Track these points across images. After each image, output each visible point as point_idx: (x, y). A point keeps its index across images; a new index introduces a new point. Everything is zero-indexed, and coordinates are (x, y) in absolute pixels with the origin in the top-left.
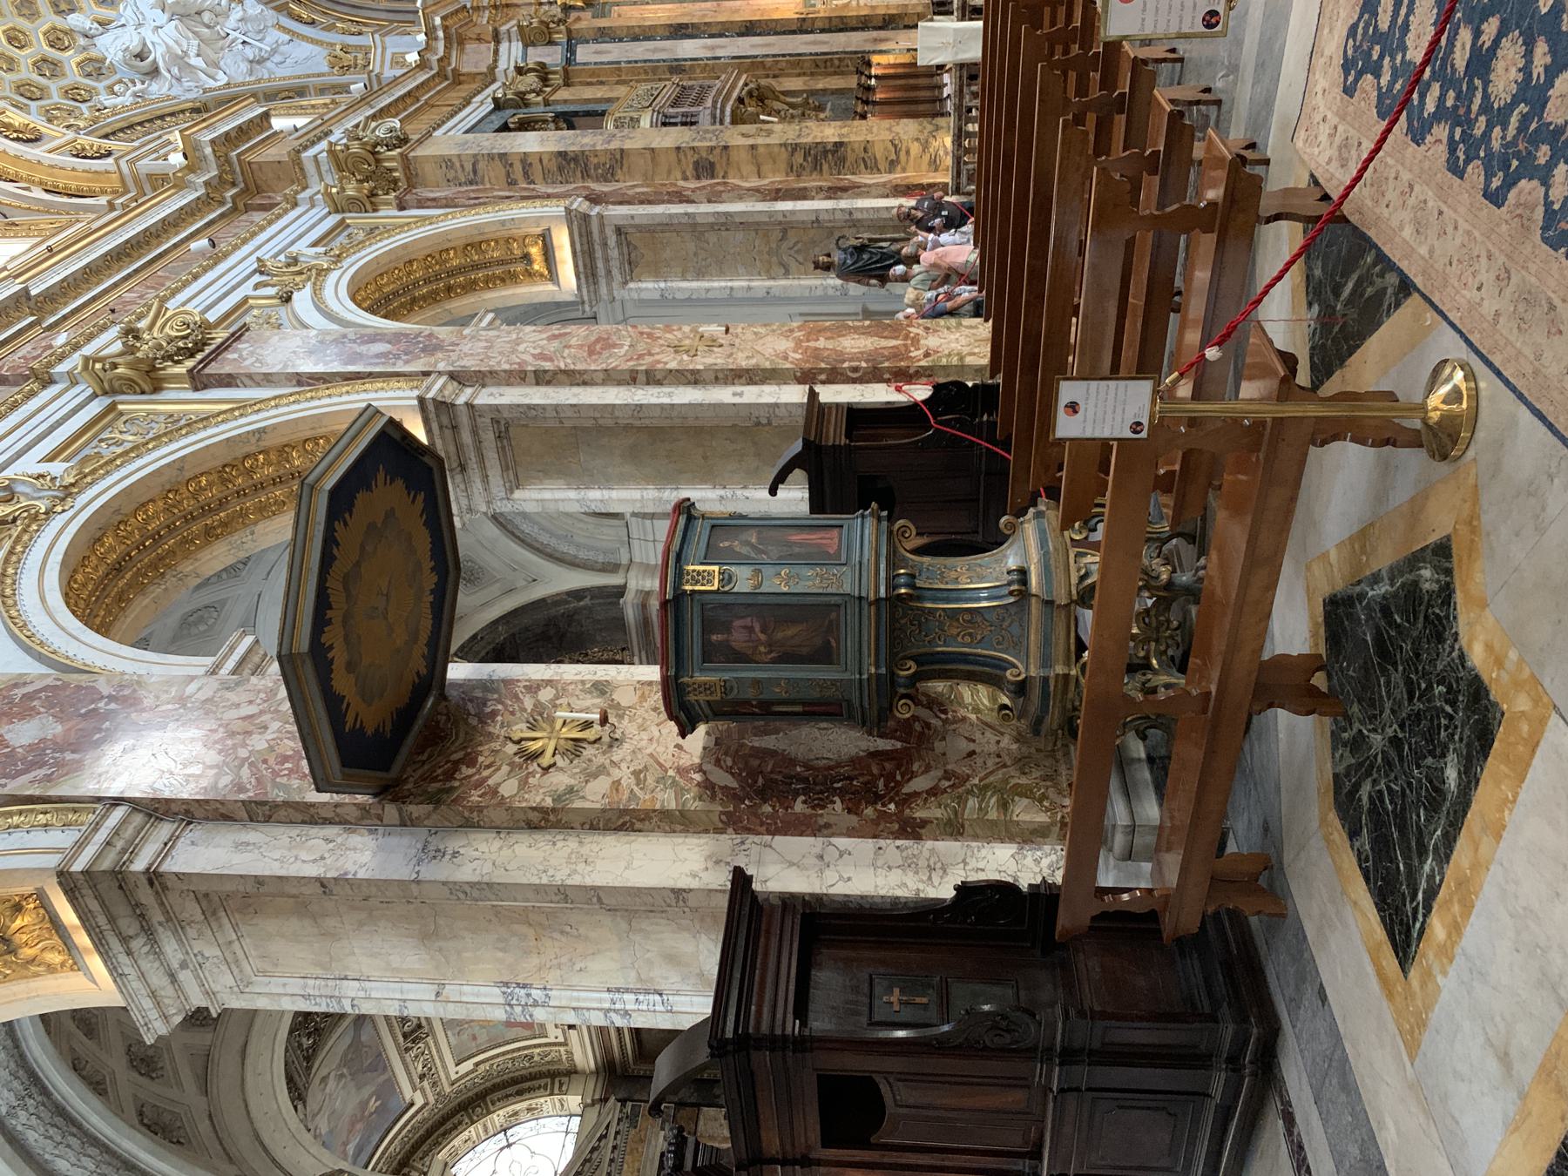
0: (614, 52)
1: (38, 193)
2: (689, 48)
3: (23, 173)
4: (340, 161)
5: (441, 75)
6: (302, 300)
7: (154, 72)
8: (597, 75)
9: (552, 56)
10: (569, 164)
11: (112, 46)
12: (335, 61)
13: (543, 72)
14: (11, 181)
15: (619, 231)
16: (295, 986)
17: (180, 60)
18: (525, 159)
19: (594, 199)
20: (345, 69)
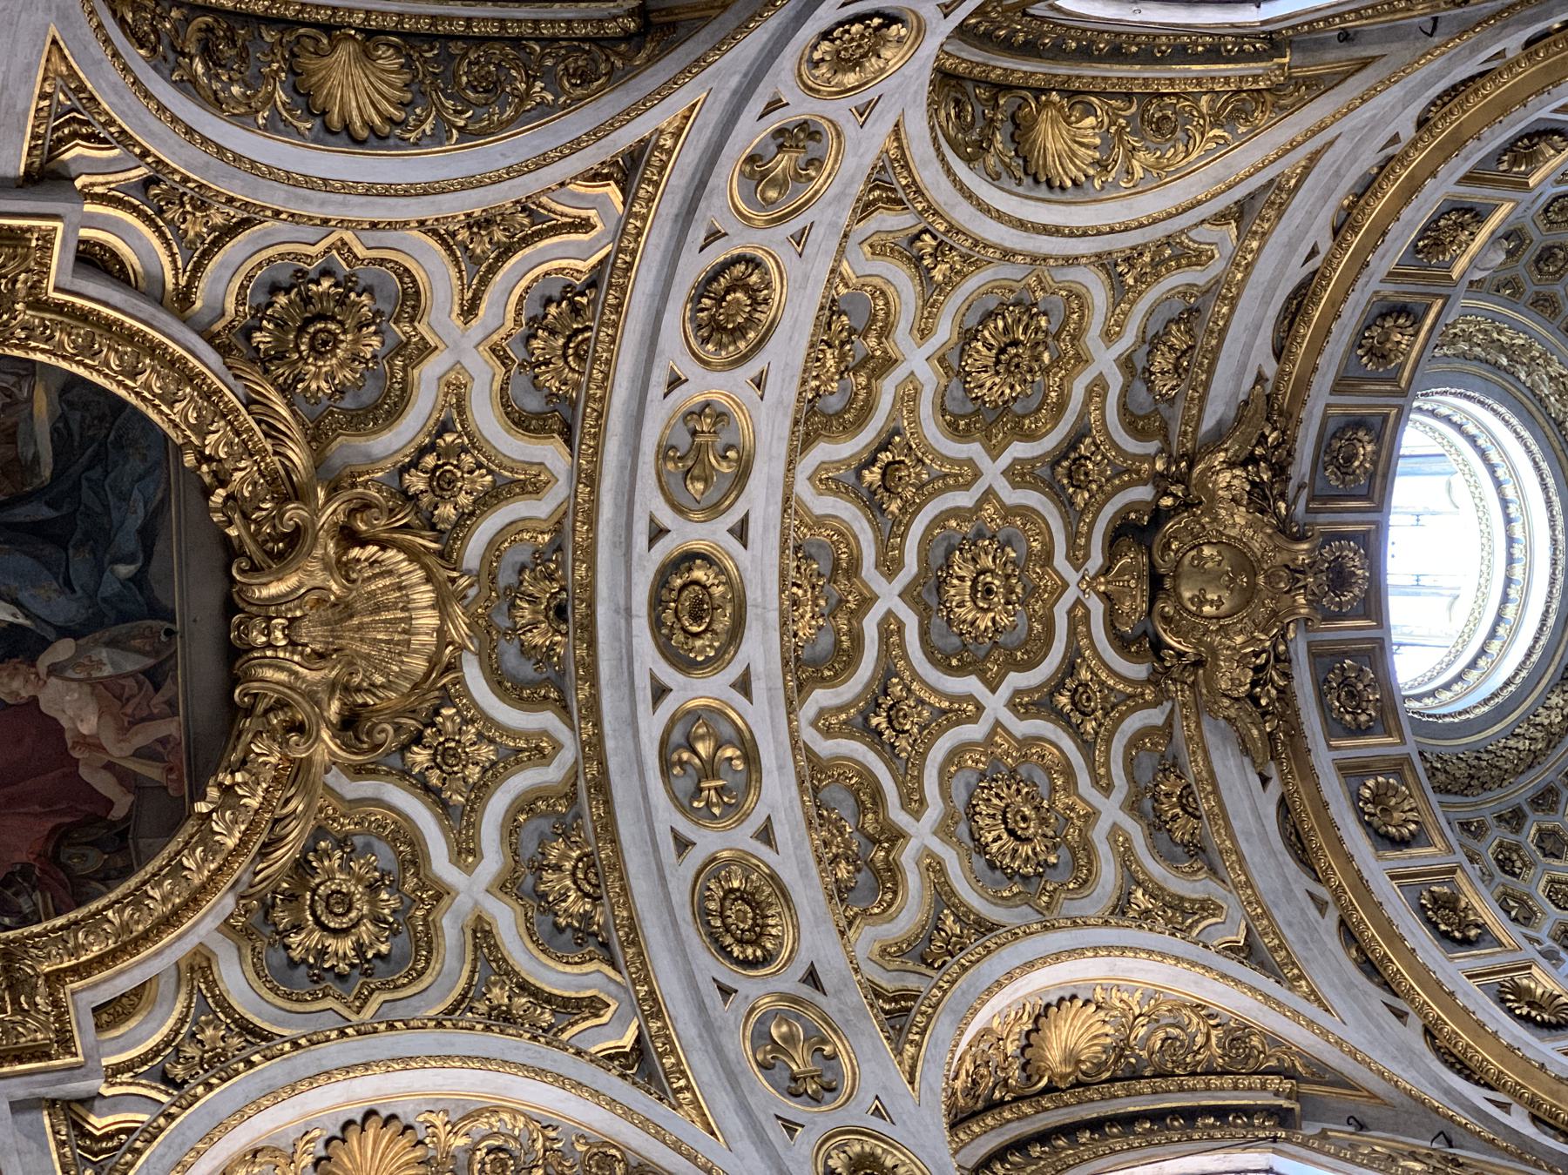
1: (1519, 1121)
3: (1511, 1077)
14: (1488, 1086)
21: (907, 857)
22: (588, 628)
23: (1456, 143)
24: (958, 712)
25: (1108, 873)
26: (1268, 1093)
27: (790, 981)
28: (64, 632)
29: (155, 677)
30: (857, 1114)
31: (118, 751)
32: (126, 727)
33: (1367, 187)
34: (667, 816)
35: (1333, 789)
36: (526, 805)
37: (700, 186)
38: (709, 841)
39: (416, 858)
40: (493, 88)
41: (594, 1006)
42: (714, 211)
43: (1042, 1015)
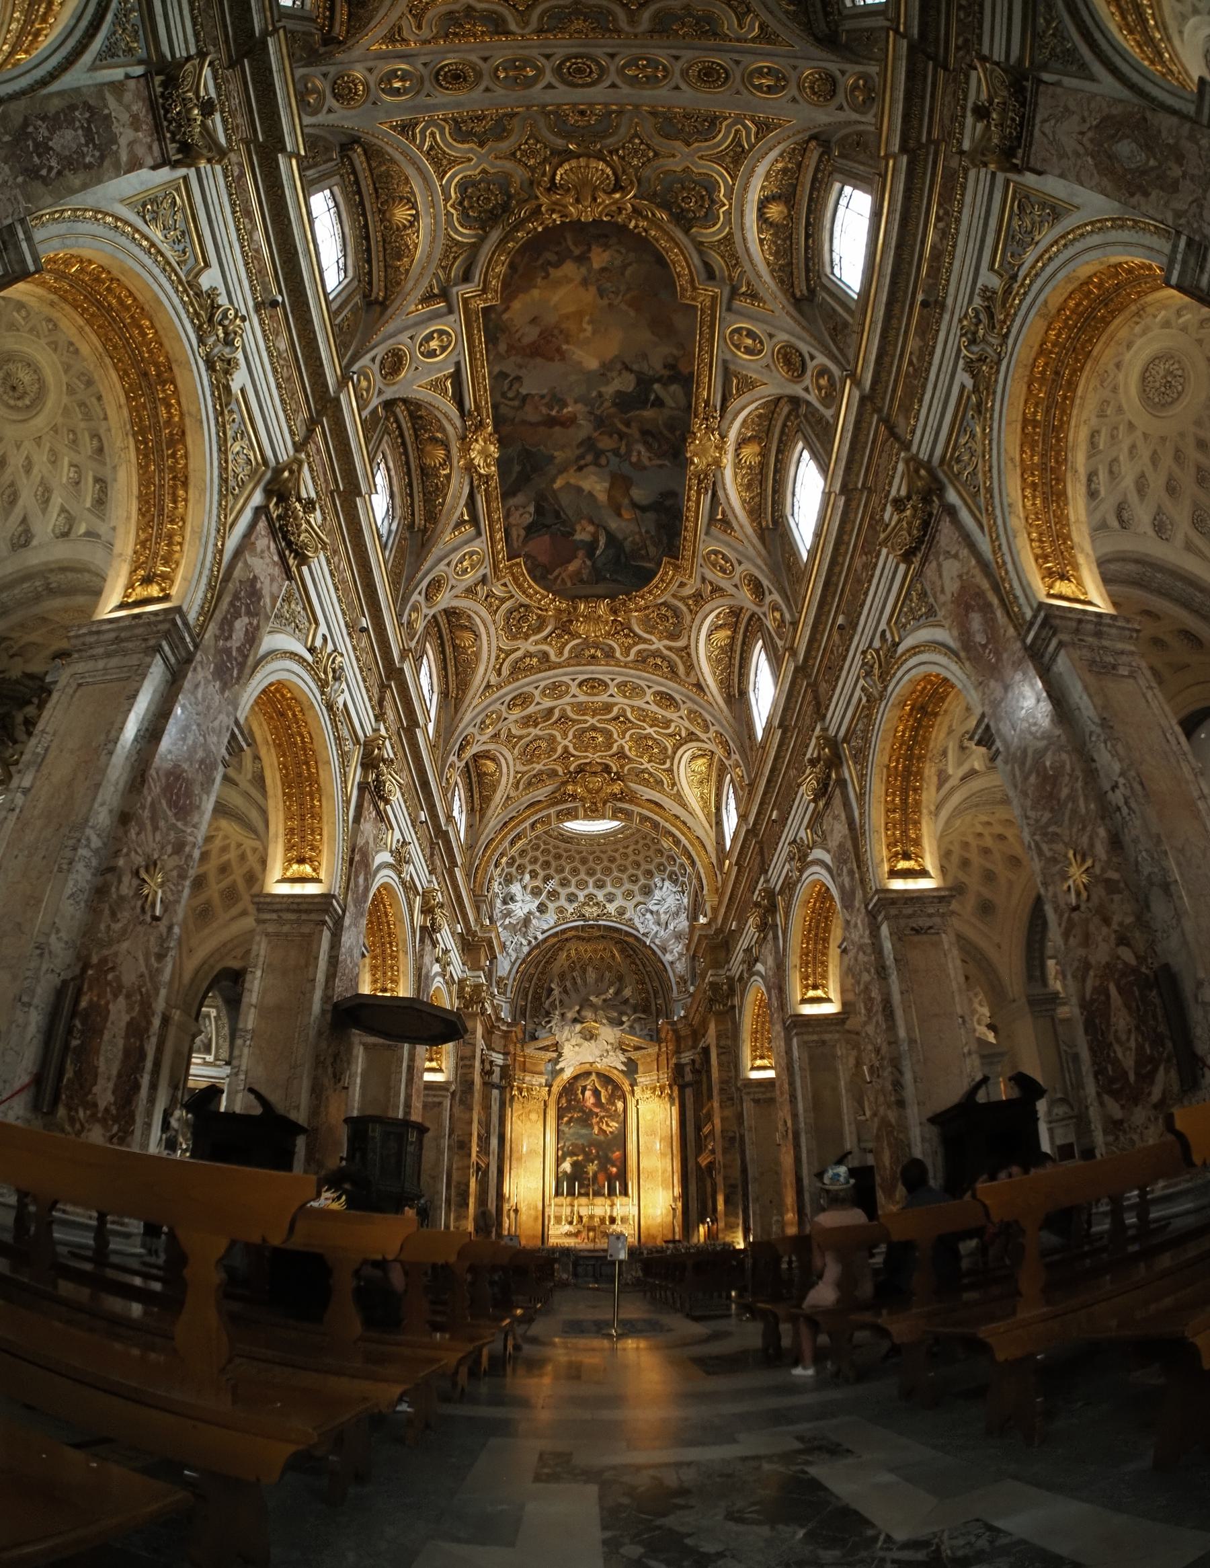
0: (495, 1107)
2: (494, 1142)
4: (477, 987)
5: (493, 1026)
6: (437, 968)
7: (505, 902)
8: (486, 1098)
9: (496, 1078)
10: (467, 1085)
11: (516, 888)
12: (501, 979)
13: (490, 1073)
15: (440, 1104)
16: (262, 952)
17: (509, 914)
18: (472, 1066)
19: (453, 1094)
20: (498, 983)
21: (531, 730)
22: (589, 664)
23: (692, 844)
24: (565, 735)
25: (525, 769)
26: (477, 807)
27: (505, 715)
28: (594, 563)
29: (581, 581)
30: (478, 737)
31: (564, 575)
32: (571, 577)
33: (684, 823)
34: (542, 684)
35: (545, 813)
36: (546, 655)
37: (695, 702)
38: (537, 693)
39: (535, 633)
40: (719, 661)
41: (499, 675)
42: (689, 704)
43: (494, 759)
